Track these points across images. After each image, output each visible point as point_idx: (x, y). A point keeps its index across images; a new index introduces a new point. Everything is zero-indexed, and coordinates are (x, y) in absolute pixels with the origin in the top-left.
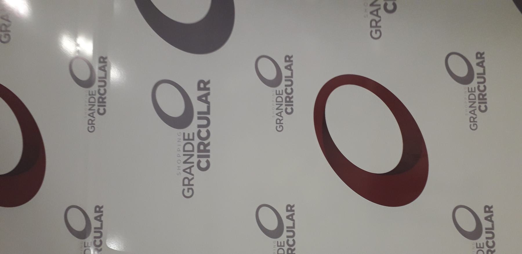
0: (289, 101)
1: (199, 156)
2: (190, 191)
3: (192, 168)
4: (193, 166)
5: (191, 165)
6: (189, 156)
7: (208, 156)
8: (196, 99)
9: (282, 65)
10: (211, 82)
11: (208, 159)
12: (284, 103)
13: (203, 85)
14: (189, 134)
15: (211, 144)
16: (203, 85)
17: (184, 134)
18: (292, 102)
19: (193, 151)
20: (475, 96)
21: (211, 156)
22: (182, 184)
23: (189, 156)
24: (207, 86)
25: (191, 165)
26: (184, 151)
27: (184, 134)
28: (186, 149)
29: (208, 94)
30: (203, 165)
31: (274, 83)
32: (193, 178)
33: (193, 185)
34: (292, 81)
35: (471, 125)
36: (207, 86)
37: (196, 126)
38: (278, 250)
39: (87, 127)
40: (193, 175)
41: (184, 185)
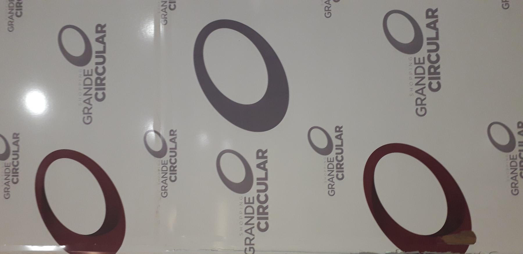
0: (340, 167)
1: (259, 218)
2: (423, 110)
3: (253, 229)
4: (253, 227)
5: (252, 226)
6: (420, 79)
7: (267, 218)
8: (255, 166)
9: (333, 135)
10: (268, 151)
11: (439, 80)
12: (335, 169)
13: (262, 154)
14: (419, 59)
15: (441, 66)
16: (262, 154)
17: (415, 58)
18: (343, 168)
19: (424, 74)
20: (517, 164)
21: (269, 218)
22: (244, 244)
23: (420, 79)
24: (435, 14)
25: (252, 226)
26: (246, 213)
27: (415, 58)
28: (247, 212)
29: (437, 21)
30: (435, 86)
31: (326, 151)
32: (425, 99)
33: (253, 244)
34: (342, 149)
35: (512, 191)
36: (435, 14)
37: (256, 191)
38: (512, 162)
39: (160, 194)
40: (425, 95)
41: (417, 105)
